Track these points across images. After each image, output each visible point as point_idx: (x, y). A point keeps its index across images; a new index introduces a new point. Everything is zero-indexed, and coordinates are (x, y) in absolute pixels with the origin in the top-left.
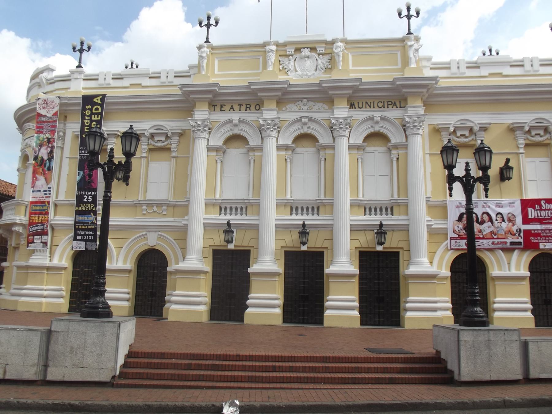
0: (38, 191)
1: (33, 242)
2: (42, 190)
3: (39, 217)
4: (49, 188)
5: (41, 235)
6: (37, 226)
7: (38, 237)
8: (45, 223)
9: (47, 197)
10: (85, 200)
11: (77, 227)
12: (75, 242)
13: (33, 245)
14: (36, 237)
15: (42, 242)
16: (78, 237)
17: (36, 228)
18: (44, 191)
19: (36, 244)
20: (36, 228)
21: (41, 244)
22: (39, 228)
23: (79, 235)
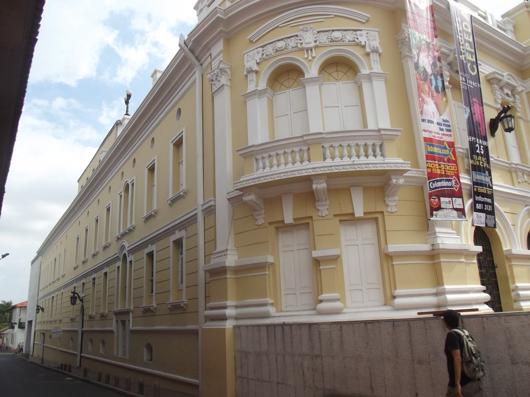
0: (429, 121)
1: (439, 208)
2: (435, 121)
3: (440, 165)
4: (444, 121)
5: (452, 197)
6: (441, 181)
7: (447, 199)
8: (452, 176)
9: (444, 134)
10: (478, 151)
11: (475, 190)
12: (475, 213)
13: (440, 212)
14: (442, 199)
15: (457, 210)
16: (479, 206)
17: (439, 184)
18: (438, 124)
19: (445, 211)
20: (439, 184)
21: (455, 212)
22: (445, 184)
23: (479, 202)
